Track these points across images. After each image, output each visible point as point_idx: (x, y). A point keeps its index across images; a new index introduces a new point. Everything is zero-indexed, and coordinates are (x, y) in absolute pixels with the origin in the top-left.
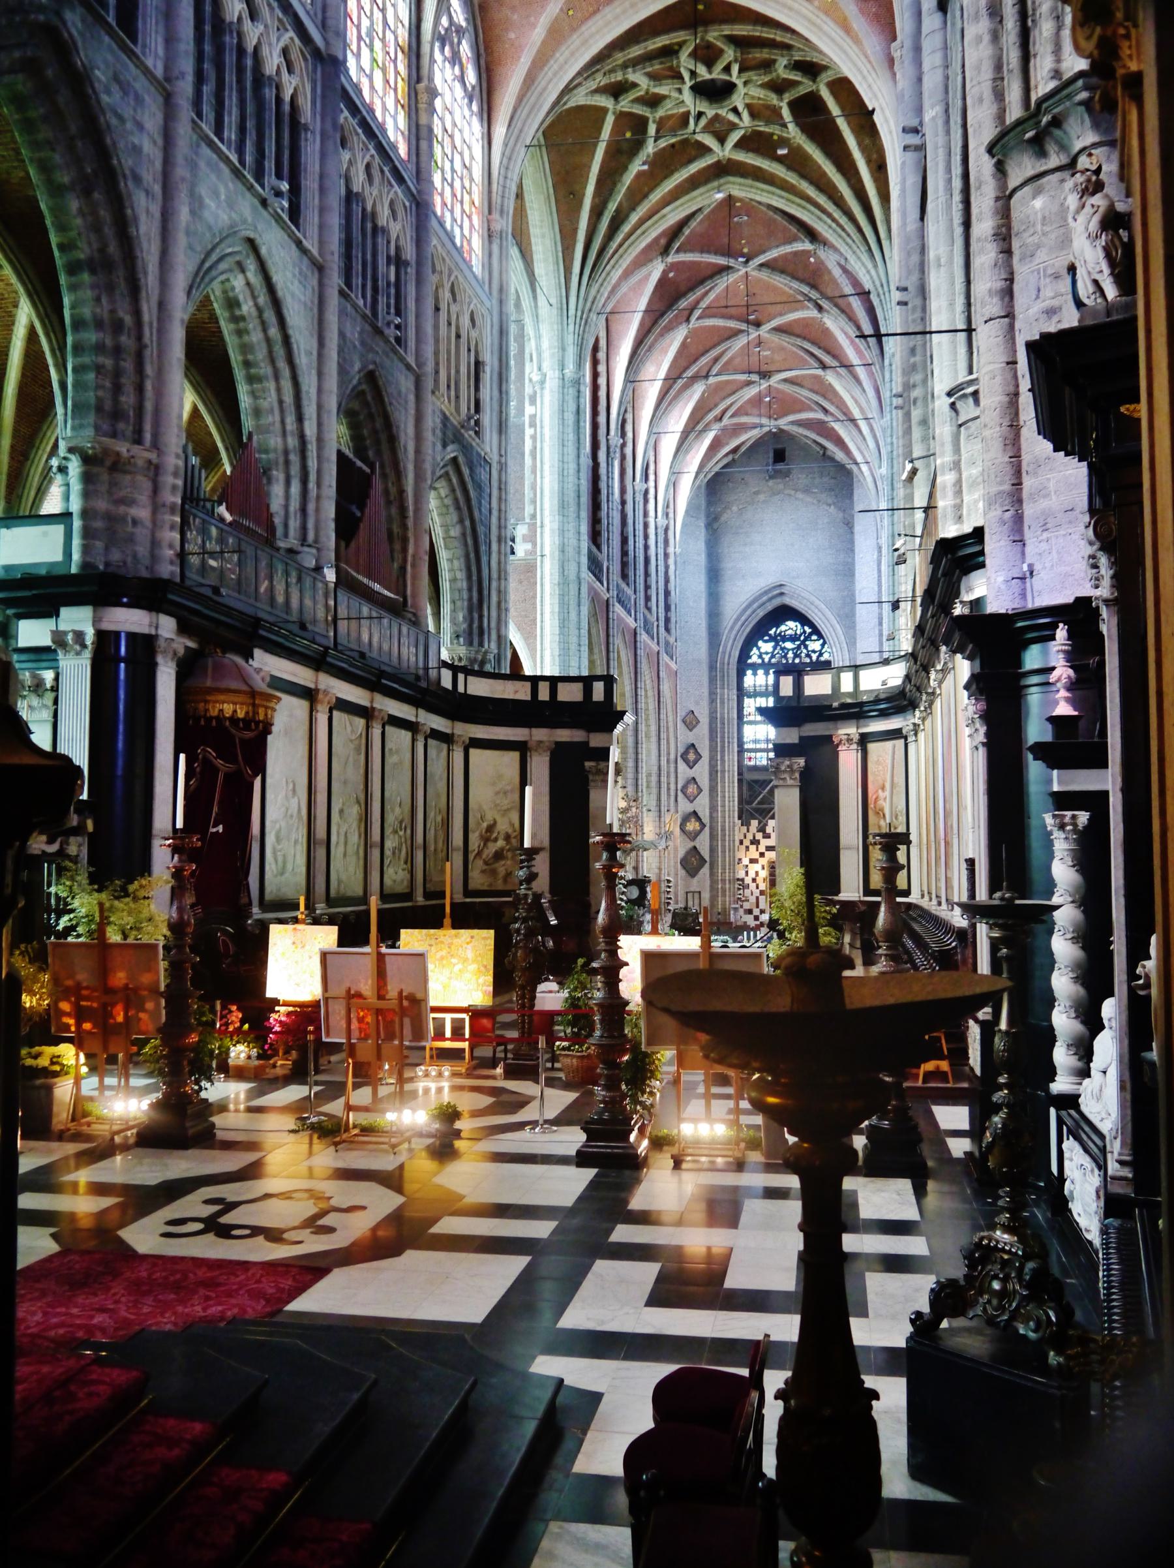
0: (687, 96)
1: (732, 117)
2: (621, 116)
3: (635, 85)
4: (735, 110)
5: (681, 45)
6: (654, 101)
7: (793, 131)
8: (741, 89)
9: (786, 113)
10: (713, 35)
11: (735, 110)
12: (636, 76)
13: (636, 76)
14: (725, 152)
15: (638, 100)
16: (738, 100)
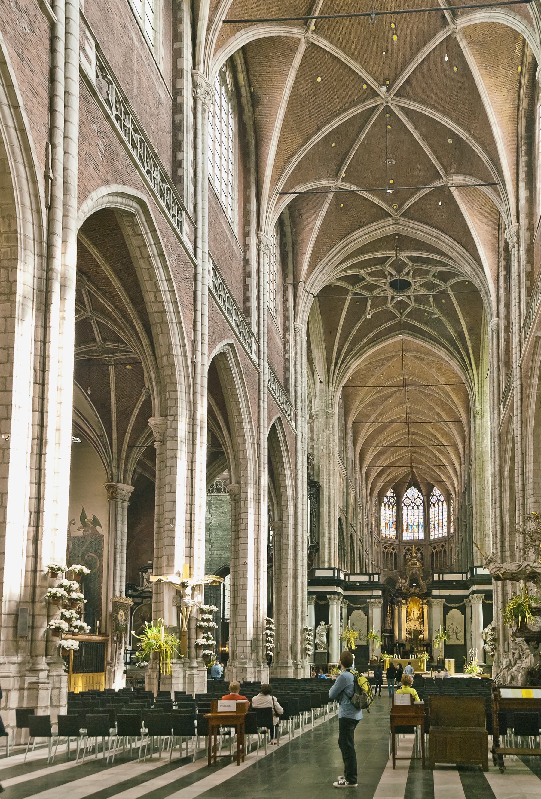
0: (387, 287)
1: (407, 300)
2: (356, 294)
3: (364, 279)
4: (409, 297)
5: (388, 258)
6: (371, 288)
7: (434, 309)
8: (413, 287)
9: (431, 299)
10: (403, 256)
11: (409, 297)
12: (364, 273)
13: (364, 273)
14: (402, 318)
15: (364, 288)
16: (411, 292)
